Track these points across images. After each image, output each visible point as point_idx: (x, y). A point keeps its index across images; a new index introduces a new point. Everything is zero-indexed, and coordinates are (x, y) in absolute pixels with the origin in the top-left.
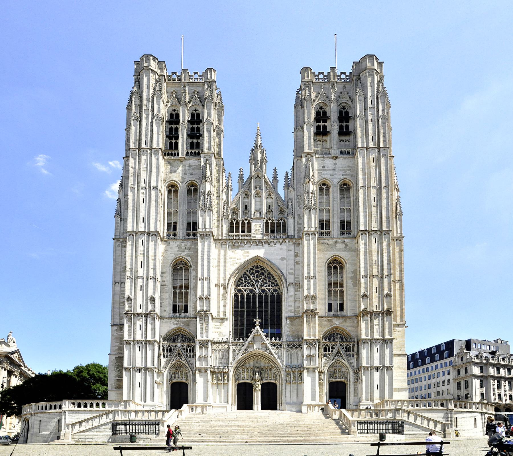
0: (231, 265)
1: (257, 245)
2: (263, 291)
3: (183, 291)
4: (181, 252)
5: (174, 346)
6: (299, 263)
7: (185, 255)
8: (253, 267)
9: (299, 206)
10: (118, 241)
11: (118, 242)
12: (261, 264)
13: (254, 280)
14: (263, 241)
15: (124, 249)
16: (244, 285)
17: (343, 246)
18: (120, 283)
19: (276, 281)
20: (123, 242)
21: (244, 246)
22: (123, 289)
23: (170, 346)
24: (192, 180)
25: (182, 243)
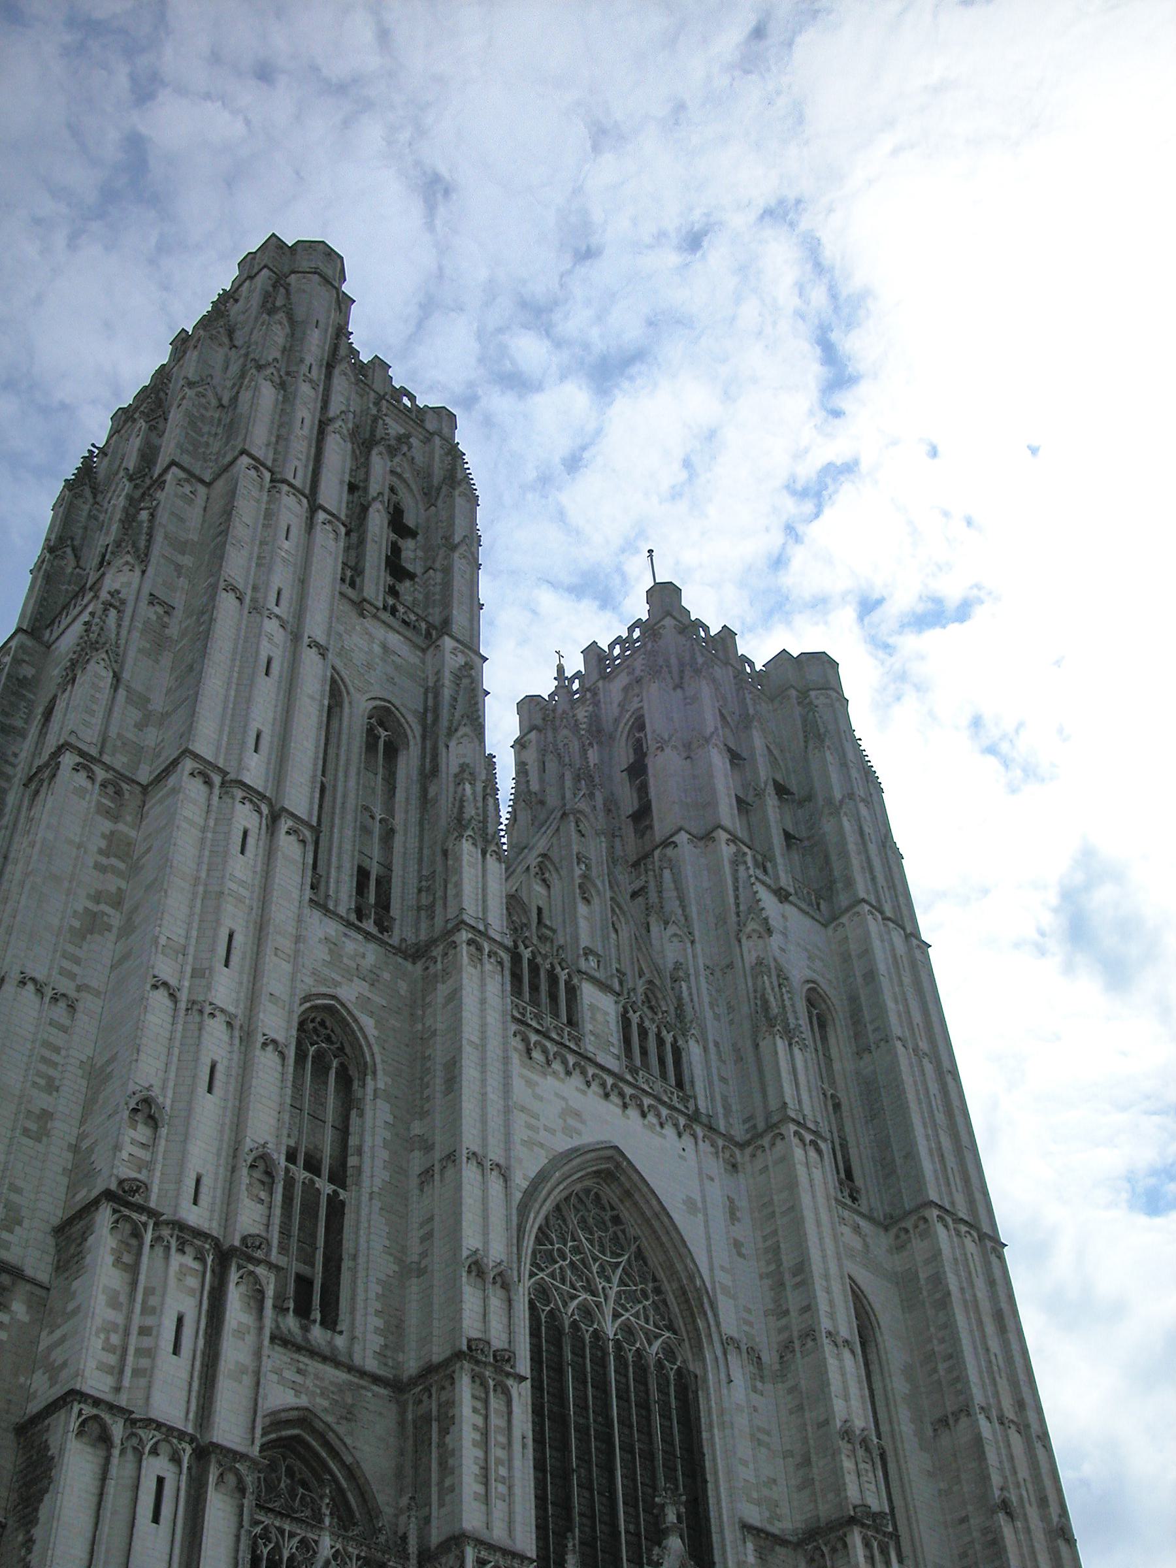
0: (524, 1142)
1: (607, 1096)
2: (628, 1330)
3: (325, 1187)
4: (338, 978)
5: (295, 1541)
6: (744, 1251)
7: (354, 1000)
8: (587, 1191)
9: (712, 1005)
10: (85, 767)
11: (83, 774)
12: (610, 1193)
13: (595, 1260)
14: (629, 1091)
15: (107, 826)
16: (557, 1266)
17: (856, 1243)
18: (49, 993)
19: (665, 1302)
20: (103, 785)
21: (562, 1075)
22: (58, 1039)
23: (274, 1535)
24: (389, 702)
25: (346, 935)
